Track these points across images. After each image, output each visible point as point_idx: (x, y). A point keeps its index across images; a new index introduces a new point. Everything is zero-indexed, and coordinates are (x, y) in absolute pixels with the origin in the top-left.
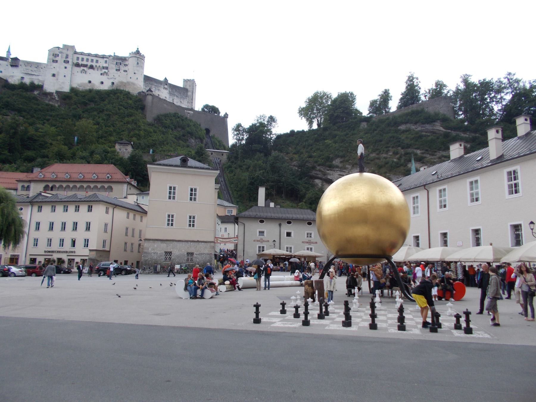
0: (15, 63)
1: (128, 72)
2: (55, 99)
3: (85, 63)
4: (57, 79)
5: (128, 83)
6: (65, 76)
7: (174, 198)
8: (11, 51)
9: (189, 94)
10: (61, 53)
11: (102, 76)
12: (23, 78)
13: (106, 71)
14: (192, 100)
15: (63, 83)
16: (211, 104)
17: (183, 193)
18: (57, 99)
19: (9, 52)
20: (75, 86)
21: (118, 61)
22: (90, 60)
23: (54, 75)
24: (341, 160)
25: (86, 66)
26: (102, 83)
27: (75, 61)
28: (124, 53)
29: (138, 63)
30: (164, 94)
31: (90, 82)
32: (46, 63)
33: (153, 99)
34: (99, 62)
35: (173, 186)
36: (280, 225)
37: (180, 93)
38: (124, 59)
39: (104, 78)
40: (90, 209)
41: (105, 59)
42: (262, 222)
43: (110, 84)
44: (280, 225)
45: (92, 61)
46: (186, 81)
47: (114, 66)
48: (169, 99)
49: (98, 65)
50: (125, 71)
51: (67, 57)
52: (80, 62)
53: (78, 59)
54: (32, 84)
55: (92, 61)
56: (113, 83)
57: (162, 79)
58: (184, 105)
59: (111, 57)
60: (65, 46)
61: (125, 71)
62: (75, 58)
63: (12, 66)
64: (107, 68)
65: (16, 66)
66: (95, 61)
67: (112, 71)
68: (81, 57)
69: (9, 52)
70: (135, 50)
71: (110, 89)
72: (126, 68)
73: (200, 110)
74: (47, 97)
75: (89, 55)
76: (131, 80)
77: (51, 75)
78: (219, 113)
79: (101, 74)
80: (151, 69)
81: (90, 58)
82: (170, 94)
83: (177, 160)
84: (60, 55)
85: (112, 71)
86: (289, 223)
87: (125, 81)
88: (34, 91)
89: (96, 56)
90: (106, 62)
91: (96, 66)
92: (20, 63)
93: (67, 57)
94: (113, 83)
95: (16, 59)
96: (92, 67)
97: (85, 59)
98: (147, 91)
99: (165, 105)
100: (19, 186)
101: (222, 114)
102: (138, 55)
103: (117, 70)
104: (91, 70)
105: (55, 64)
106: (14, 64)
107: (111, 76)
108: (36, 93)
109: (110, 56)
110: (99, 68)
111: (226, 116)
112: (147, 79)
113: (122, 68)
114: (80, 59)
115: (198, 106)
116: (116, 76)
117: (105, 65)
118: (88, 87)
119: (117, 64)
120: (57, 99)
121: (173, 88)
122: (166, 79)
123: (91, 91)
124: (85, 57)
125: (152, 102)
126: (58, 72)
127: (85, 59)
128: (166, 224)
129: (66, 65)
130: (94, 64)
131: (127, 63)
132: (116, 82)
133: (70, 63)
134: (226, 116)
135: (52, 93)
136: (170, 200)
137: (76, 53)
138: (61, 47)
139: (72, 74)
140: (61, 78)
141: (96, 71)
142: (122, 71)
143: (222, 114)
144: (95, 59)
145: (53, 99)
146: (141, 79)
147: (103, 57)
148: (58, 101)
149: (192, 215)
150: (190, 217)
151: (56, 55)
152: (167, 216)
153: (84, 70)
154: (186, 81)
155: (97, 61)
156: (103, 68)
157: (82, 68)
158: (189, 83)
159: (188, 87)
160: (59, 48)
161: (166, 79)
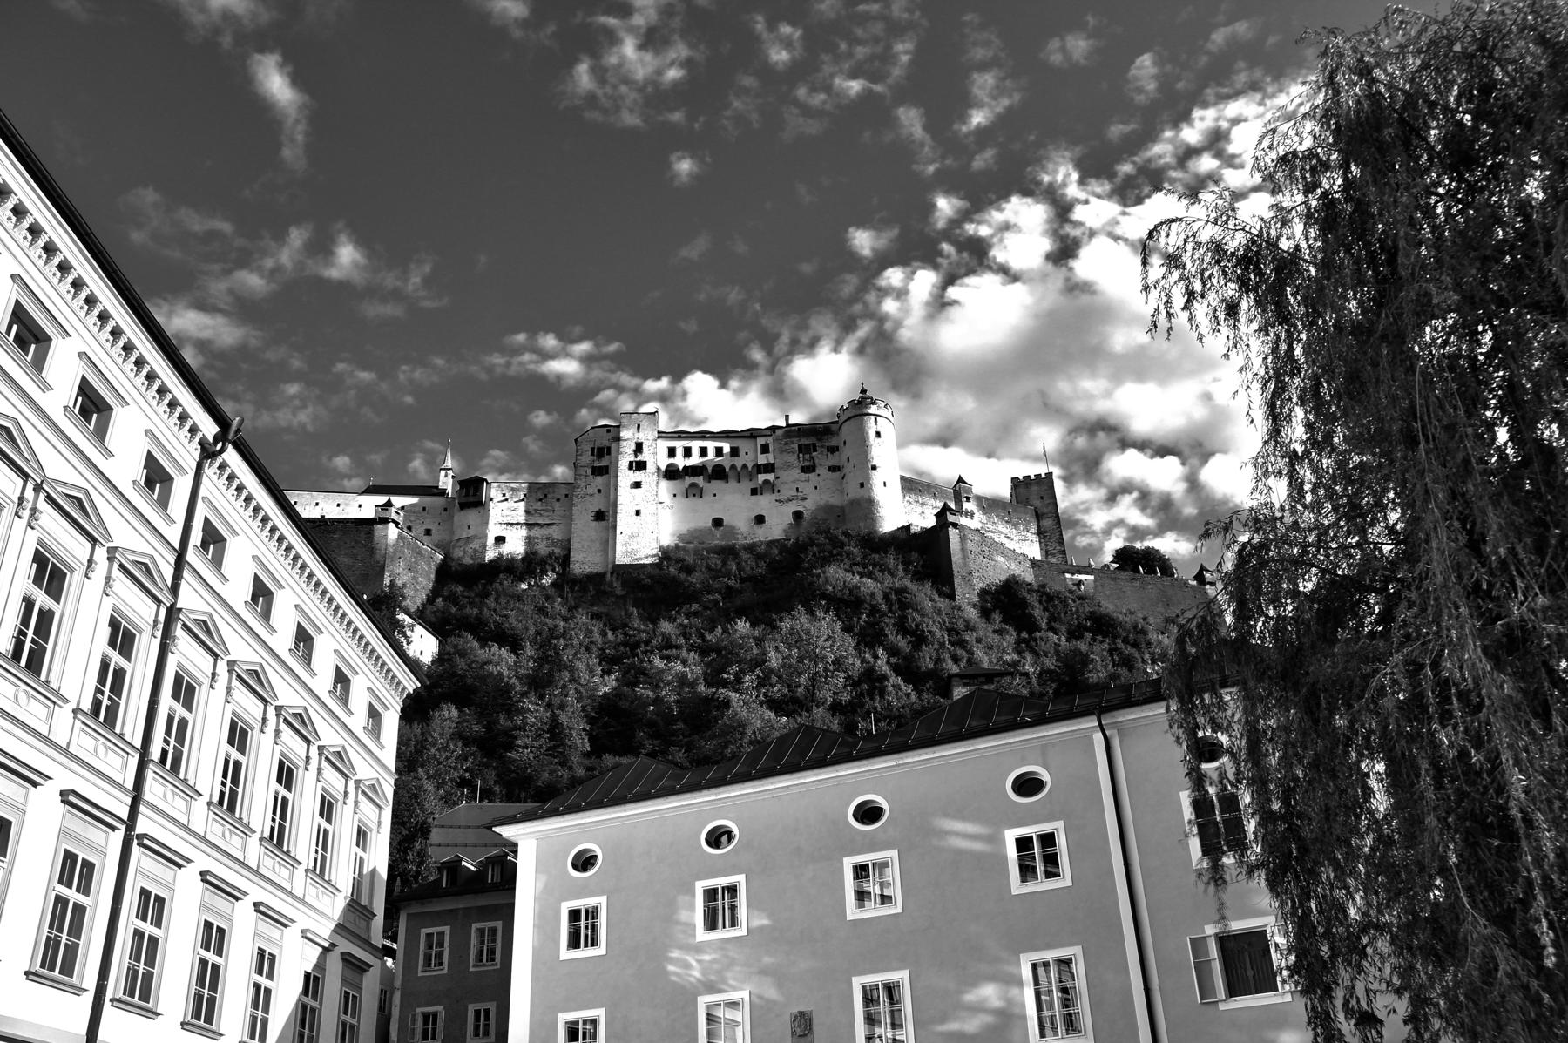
1: (848, 468)
2: (611, 594)
6: (638, 513)
11: (759, 497)
13: (771, 477)
18: (619, 592)
21: (805, 441)
23: (600, 516)
26: (760, 520)
27: (664, 462)
31: (718, 522)
33: (963, 539)
34: (742, 453)
37: (1016, 526)
39: (764, 504)
41: (761, 441)
43: (790, 519)
45: (719, 451)
47: (792, 459)
49: (739, 462)
51: (639, 448)
52: (680, 461)
53: (672, 452)
56: (798, 515)
59: (779, 432)
62: (666, 452)
64: (769, 468)
67: (791, 478)
68: (679, 445)
72: (833, 460)
74: (584, 590)
77: (590, 517)
79: (754, 492)
84: (614, 446)
87: (835, 500)
90: (765, 449)
91: (733, 467)
96: (718, 473)
99: (1001, 559)
103: (805, 470)
104: (717, 485)
105: (599, 480)
106: (471, 499)
107: (786, 492)
109: (773, 428)
110: (740, 474)
113: (823, 460)
114: (680, 452)
116: (807, 489)
117: (762, 460)
118: (718, 539)
119: (800, 451)
120: (619, 592)
123: (728, 552)
125: (963, 550)
131: (833, 442)
132: (808, 507)
133: (651, 467)
141: (733, 484)
142: (822, 470)
145: (605, 593)
147: (752, 434)
148: (623, 597)
153: (693, 485)
156: (761, 469)
157: (688, 480)
158: (1035, 488)
161: (960, 480)
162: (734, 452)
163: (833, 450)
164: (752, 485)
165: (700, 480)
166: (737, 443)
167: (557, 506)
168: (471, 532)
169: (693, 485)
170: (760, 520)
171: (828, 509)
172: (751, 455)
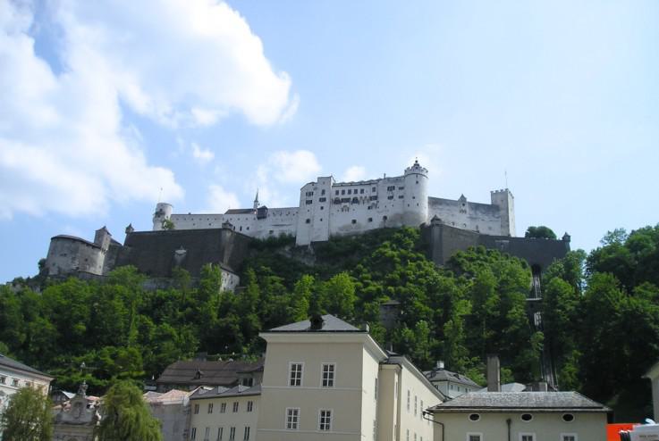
0: (262, 213)
1: (405, 197)
3: (346, 196)
4: (312, 226)
5: (405, 213)
7: (298, 383)
8: (259, 200)
9: (502, 212)
10: (315, 189)
12: (271, 232)
13: (375, 202)
14: (508, 221)
15: (319, 229)
16: (537, 225)
17: (312, 376)
19: (256, 201)
20: (334, 231)
22: (353, 191)
23: (308, 221)
24: (448, 293)
25: (347, 200)
26: (371, 220)
27: (334, 197)
28: (398, 172)
29: (417, 182)
30: (461, 221)
31: (354, 222)
32: (298, 206)
33: (441, 231)
35: (297, 363)
36: (509, 422)
38: (397, 179)
39: (372, 213)
40: (250, 409)
42: (474, 417)
43: (381, 220)
44: (509, 422)
45: (356, 191)
46: (494, 194)
48: (470, 227)
49: (363, 196)
50: (401, 197)
51: (323, 192)
52: (341, 197)
53: (337, 193)
54: (282, 235)
55: (356, 191)
56: (385, 218)
57: (456, 198)
58: (495, 231)
60: (319, 178)
61: (401, 197)
63: (259, 218)
64: (376, 198)
65: (264, 217)
66: (359, 191)
69: (256, 201)
70: (411, 164)
71: (383, 227)
73: (523, 236)
75: (352, 184)
76: (409, 209)
78: (554, 236)
80: (438, 185)
81: (353, 189)
82: (472, 218)
83: (307, 324)
85: (383, 200)
86: (527, 417)
88: (284, 247)
89: (361, 183)
90: (374, 190)
92: (269, 213)
93: (323, 192)
94: (385, 218)
95: (264, 209)
96: (355, 201)
97: (347, 192)
98: (432, 221)
99: (462, 237)
100: (242, 377)
101: (559, 237)
102: (416, 171)
107: (381, 208)
108: (287, 249)
109: (378, 180)
111: (567, 238)
112: (434, 202)
113: (397, 193)
114: (340, 192)
115: (518, 230)
116: (389, 207)
118: (353, 229)
121: (476, 207)
122: (463, 196)
123: (356, 235)
124: (346, 189)
126: (313, 217)
127: (347, 192)
128: (286, 425)
129: (322, 204)
130: (359, 195)
132: (389, 215)
133: (327, 200)
134: (567, 238)
135: (307, 246)
136: (293, 387)
137: (335, 185)
138: (316, 181)
139: (331, 215)
140: (316, 223)
141: (361, 204)
143: (559, 237)
144: (359, 189)
146: (425, 203)
149: (326, 410)
150: (323, 414)
151: (310, 194)
152: (287, 412)
154: (494, 194)
155: (362, 191)
156: (371, 198)
157: (343, 204)
159: (499, 203)
160: (313, 183)
161: (463, 196)
162: (362, 191)
163: (401, 188)
164: (370, 205)
165: (347, 204)
166: (362, 187)
167: (293, 217)
168: (263, 228)
169: (345, 206)
170: (371, 220)
171: (397, 214)
172: (368, 192)
